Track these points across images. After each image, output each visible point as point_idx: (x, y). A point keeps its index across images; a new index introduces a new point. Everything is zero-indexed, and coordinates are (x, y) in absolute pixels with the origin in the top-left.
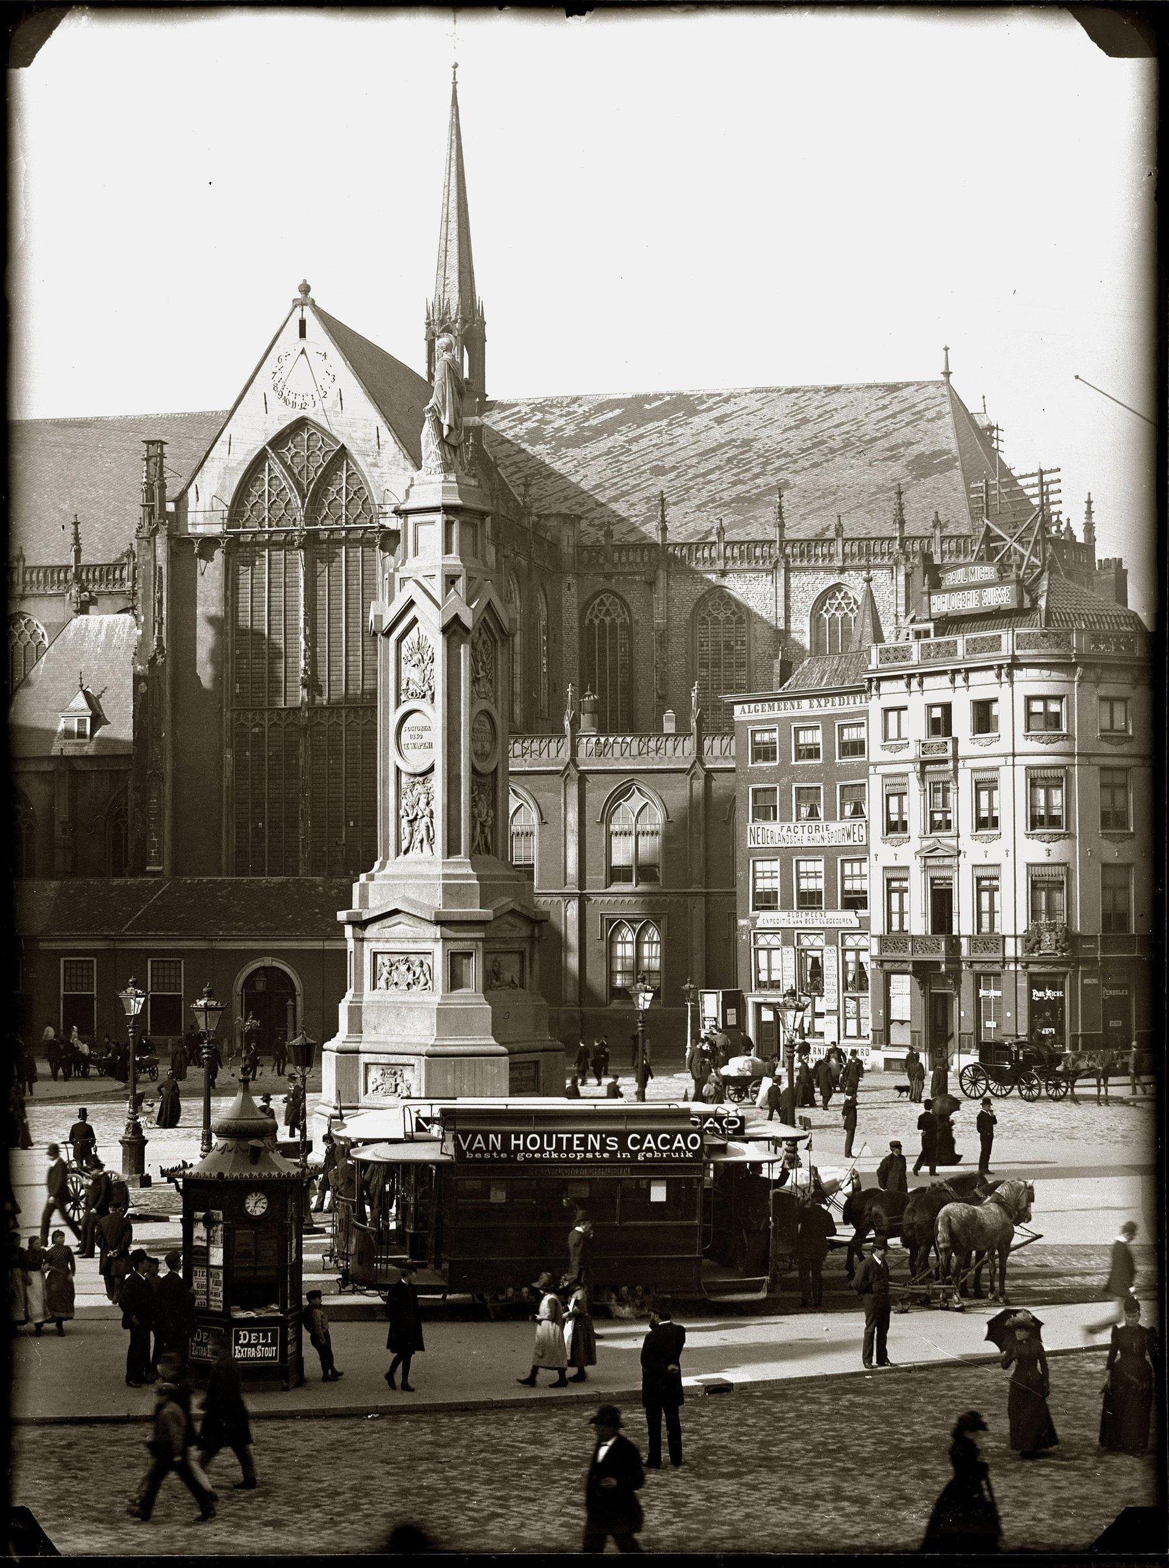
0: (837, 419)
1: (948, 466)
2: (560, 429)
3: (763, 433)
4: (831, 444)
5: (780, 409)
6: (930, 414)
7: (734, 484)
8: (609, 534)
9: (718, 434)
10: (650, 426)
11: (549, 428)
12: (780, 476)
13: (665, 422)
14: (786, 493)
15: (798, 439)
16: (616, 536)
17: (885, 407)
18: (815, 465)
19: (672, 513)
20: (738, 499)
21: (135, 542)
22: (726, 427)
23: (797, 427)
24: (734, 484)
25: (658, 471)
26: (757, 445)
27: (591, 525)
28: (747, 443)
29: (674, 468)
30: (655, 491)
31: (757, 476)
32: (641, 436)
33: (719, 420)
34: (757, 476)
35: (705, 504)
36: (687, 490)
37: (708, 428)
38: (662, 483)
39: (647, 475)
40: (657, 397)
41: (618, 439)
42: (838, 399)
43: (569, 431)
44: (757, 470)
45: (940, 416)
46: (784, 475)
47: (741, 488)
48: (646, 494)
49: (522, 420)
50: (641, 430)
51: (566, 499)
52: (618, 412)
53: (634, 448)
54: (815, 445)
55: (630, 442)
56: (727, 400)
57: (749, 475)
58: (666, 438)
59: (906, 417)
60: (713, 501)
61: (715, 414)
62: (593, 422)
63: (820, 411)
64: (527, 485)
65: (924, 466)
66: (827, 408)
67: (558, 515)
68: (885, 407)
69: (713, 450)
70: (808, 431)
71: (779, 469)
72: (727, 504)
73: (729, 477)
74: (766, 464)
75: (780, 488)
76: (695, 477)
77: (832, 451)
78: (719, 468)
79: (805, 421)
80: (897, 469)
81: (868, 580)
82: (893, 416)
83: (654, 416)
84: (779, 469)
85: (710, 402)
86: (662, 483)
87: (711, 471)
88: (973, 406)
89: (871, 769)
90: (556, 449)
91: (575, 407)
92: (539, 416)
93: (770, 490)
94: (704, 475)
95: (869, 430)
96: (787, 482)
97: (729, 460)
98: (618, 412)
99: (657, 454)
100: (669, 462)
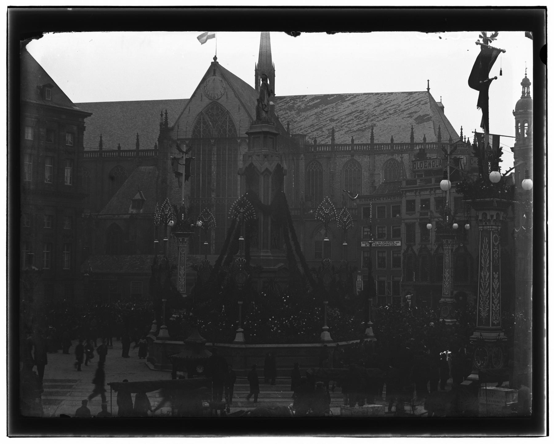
0: (392, 103)
1: (429, 119)
2: (299, 106)
3: (367, 108)
4: (391, 112)
5: (372, 100)
6: (422, 103)
8: (315, 141)
9: (352, 108)
10: (329, 106)
11: (296, 106)
12: (373, 122)
13: (334, 104)
14: (375, 128)
15: (378, 111)
16: (318, 142)
17: (408, 100)
18: (384, 119)
19: (336, 134)
20: (358, 130)
21: (157, 143)
22: (355, 106)
23: (378, 106)
24: (357, 125)
25: (332, 120)
26: (365, 112)
27: (309, 138)
28: (362, 111)
29: (337, 120)
31: (365, 122)
32: (327, 109)
33: (353, 103)
34: (365, 122)
35: (348, 131)
36: (342, 127)
37: (348, 106)
38: (334, 124)
39: (329, 122)
40: (332, 95)
41: (319, 110)
42: (392, 97)
43: (303, 106)
45: (426, 103)
46: (374, 122)
47: (359, 126)
48: (328, 128)
49: (287, 103)
50: (326, 107)
51: (301, 129)
52: (319, 100)
53: (324, 112)
54: (385, 112)
55: (323, 110)
56: (355, 97)
57: (362, 122)
58: (334, 109)
59: (415, 103)
60: (350, 130)
61: (352, 101)
62: (310, 104)
63: (386, 101)
64: (288, 125)
65: (422, 119)
66: (389, 100)
67: (299, 135)
68: (408, 100)
69: (351, 113)
70: (383, 107)
71: (372, 120)
72: (355, 132)
73: (355, 123)
74: (368, 118)
76: (345, 122)
77: (390, 114)
78: (353, 119)
79: (381, 104)
80: (411, 121)
82: (411, 103)
83: (332, 102)
84: (372, 120)
85: (350, 98)
88: (437, 100)
89: (403, 221)
91: (304, 99)
92: (293, 101)
93: (369, 128)
94: (347, 122)
95: (403, 107)
96: (375, 125)
97: (355, 117)
98: (319, 100)
99: (331, 115)
100: (336, 118)
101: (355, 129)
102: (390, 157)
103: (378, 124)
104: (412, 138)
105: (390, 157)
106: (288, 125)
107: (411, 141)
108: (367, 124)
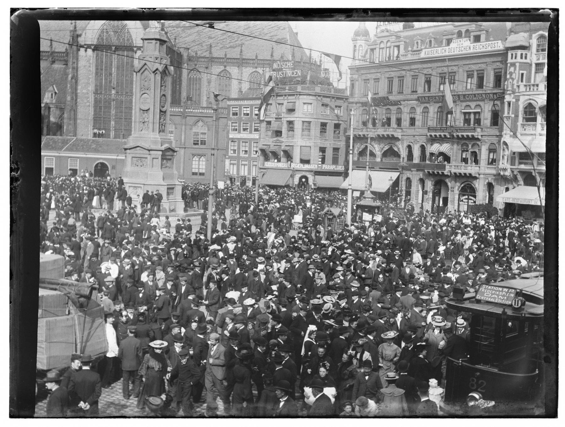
6: (282, 28)
7: (230, 43)
8: (196, 54)
24: (230, 43)
25: (210, 38)
30: (209, 43)
31: (236, 41)
34: (236, 41)
35: (222, 48)
36: (218, 43)
44: (236, 39)
47: (232, 44)
57: (233, 41)
64: (175, 39)
75: (241, 45)
81: (263, 71)
86: (211, 41)
87: (224, 39)
90: (183, 30)
96: (243, 44)
101: (228, 46)
102: (254, 70)
103: (246, 43)
104: (272, 56)
105: (254, 70)
106: (175, 39)
107: (532, 36)
108: (237, 42)
